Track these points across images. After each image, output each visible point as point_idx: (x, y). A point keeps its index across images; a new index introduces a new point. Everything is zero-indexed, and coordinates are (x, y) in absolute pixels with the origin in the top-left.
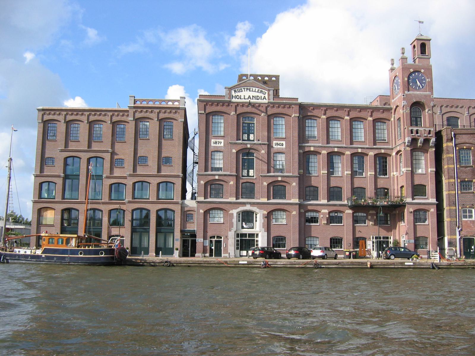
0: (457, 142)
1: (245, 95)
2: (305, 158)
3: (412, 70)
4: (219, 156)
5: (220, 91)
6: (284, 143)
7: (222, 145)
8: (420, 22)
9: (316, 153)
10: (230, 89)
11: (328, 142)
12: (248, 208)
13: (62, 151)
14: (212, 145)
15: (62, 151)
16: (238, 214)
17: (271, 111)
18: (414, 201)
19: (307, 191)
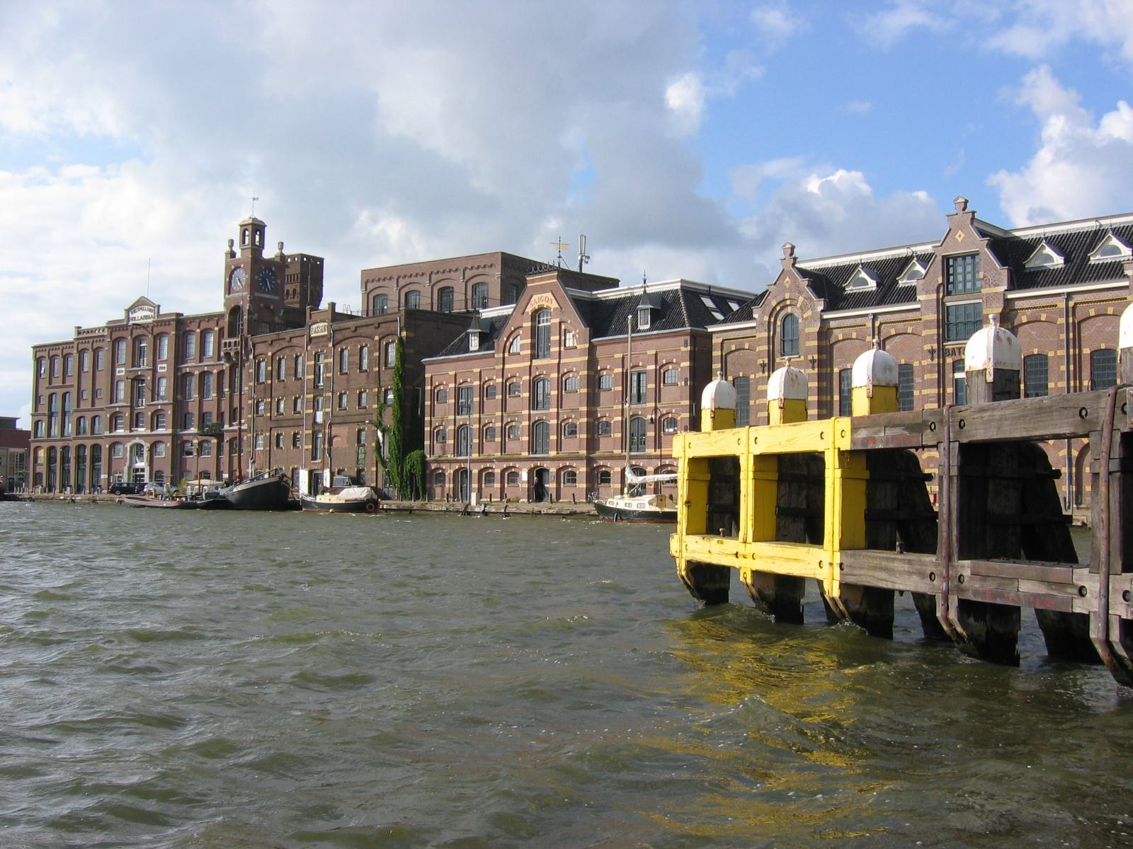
0: (256, 354)
1: (139, 316)
2: (180, 381)
3: (233, 267)
4: (122, 386)
5: (120, 315)
6: (165, 365)
7: (123, 374)
8: (254, 199)
9: (191, 374)
10: (128, 311)
11: (201, 361)
12: (137, 440)
13: (47, 388)
14: (117, 374)
15: (47, 388)
16: (131, 447)
17: (156, 330)
18: (231, 428)
19: (181, 420)
